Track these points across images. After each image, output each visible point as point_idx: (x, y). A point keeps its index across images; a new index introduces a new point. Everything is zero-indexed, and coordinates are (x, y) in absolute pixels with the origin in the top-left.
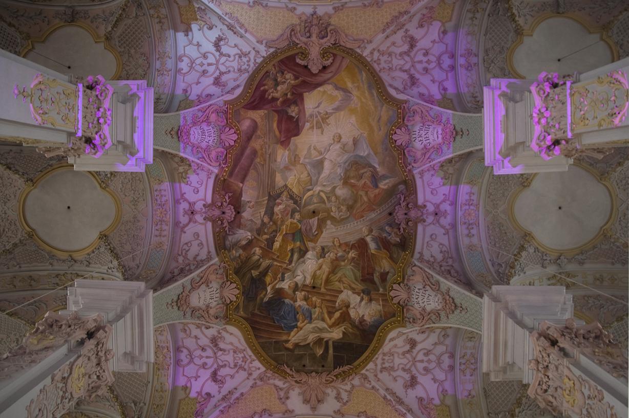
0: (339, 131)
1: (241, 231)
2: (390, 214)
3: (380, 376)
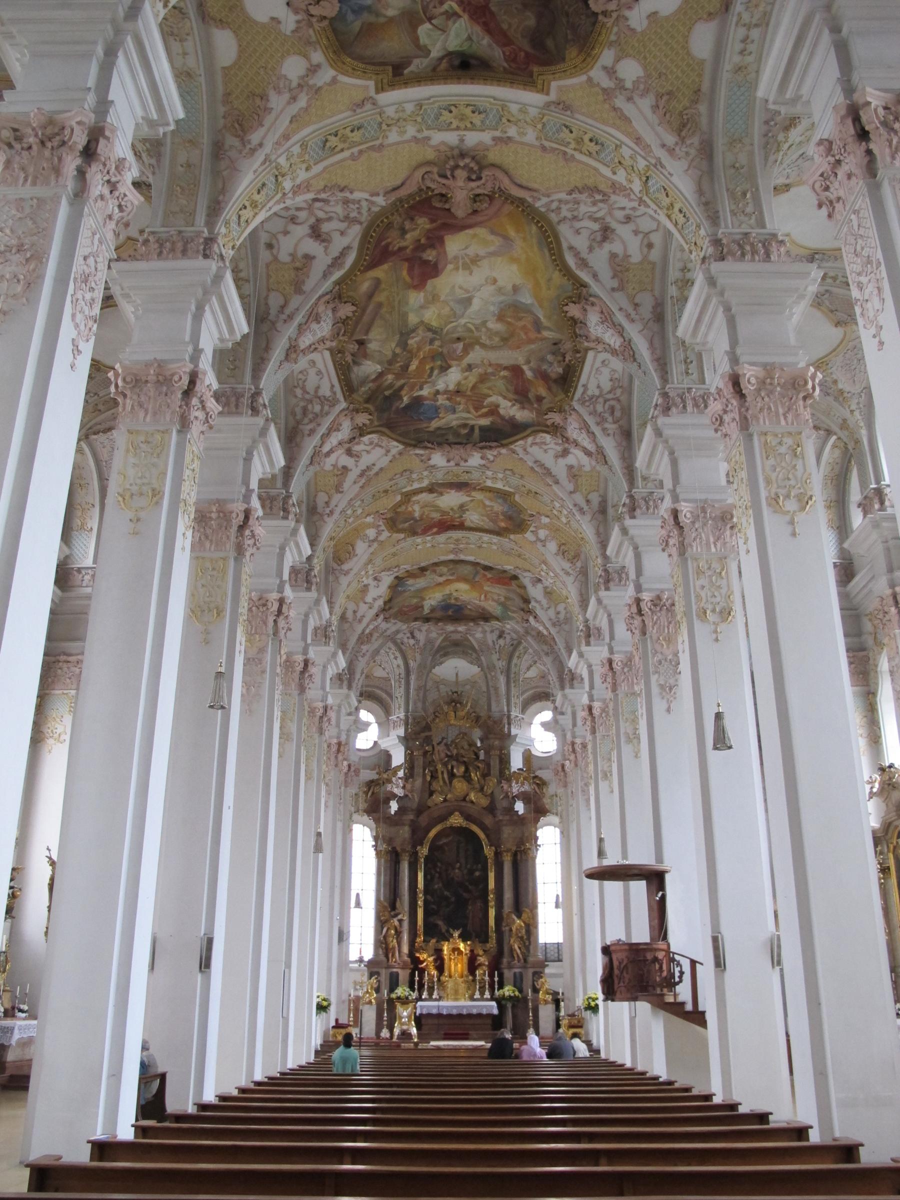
0: (495, 274)
1: (369, 363)
2: (555, 344)
3: (529, 449)
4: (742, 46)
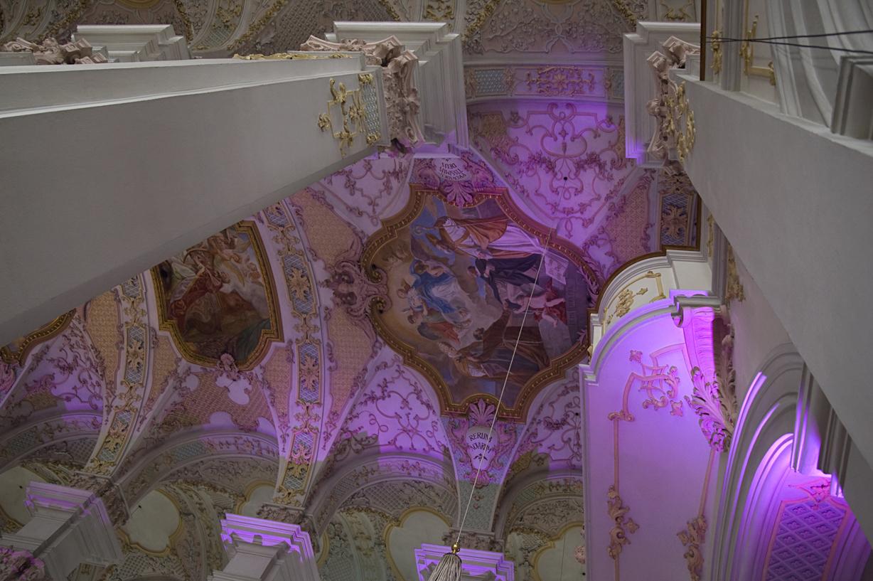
4: (224, 442)
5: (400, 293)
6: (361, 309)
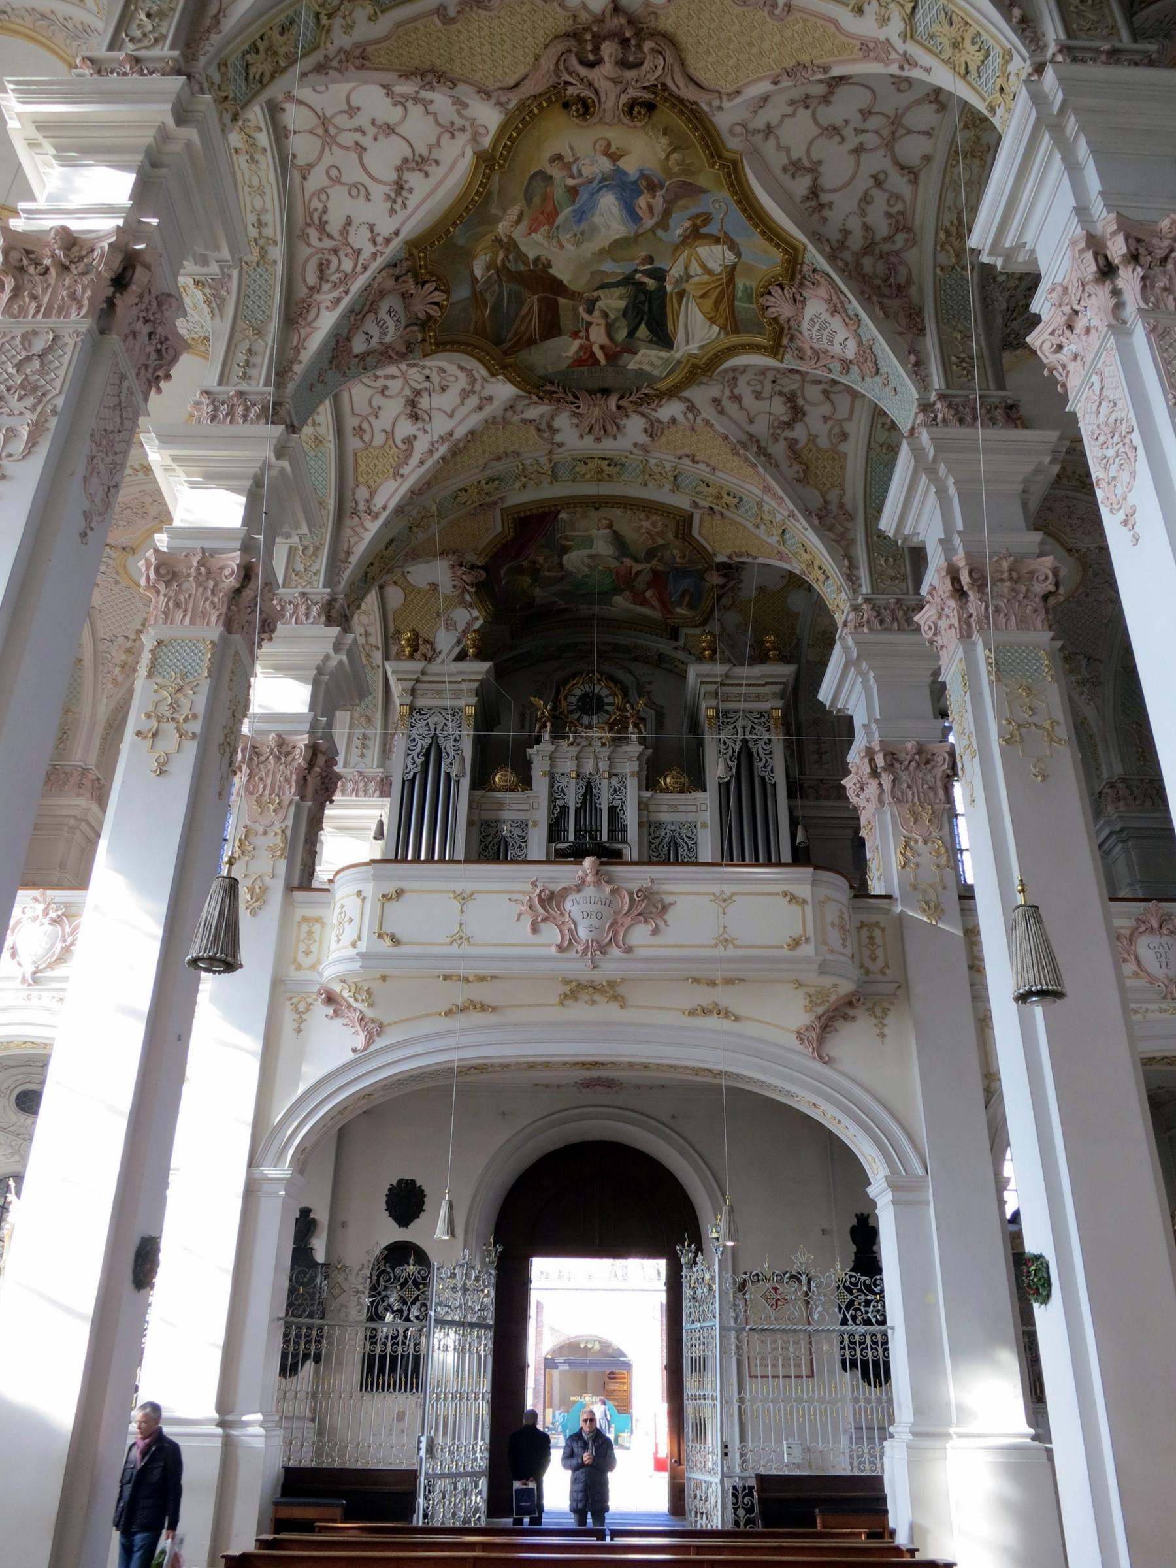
5: (604, 143)
6: (570, 74)
